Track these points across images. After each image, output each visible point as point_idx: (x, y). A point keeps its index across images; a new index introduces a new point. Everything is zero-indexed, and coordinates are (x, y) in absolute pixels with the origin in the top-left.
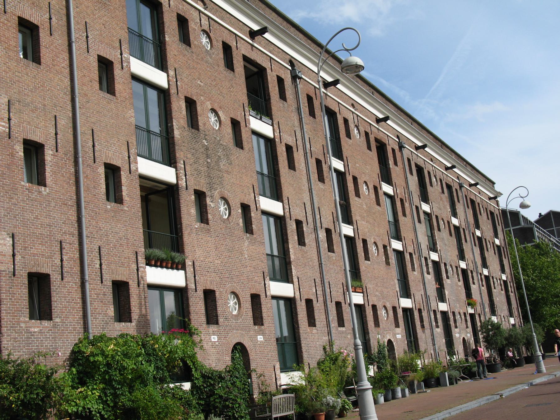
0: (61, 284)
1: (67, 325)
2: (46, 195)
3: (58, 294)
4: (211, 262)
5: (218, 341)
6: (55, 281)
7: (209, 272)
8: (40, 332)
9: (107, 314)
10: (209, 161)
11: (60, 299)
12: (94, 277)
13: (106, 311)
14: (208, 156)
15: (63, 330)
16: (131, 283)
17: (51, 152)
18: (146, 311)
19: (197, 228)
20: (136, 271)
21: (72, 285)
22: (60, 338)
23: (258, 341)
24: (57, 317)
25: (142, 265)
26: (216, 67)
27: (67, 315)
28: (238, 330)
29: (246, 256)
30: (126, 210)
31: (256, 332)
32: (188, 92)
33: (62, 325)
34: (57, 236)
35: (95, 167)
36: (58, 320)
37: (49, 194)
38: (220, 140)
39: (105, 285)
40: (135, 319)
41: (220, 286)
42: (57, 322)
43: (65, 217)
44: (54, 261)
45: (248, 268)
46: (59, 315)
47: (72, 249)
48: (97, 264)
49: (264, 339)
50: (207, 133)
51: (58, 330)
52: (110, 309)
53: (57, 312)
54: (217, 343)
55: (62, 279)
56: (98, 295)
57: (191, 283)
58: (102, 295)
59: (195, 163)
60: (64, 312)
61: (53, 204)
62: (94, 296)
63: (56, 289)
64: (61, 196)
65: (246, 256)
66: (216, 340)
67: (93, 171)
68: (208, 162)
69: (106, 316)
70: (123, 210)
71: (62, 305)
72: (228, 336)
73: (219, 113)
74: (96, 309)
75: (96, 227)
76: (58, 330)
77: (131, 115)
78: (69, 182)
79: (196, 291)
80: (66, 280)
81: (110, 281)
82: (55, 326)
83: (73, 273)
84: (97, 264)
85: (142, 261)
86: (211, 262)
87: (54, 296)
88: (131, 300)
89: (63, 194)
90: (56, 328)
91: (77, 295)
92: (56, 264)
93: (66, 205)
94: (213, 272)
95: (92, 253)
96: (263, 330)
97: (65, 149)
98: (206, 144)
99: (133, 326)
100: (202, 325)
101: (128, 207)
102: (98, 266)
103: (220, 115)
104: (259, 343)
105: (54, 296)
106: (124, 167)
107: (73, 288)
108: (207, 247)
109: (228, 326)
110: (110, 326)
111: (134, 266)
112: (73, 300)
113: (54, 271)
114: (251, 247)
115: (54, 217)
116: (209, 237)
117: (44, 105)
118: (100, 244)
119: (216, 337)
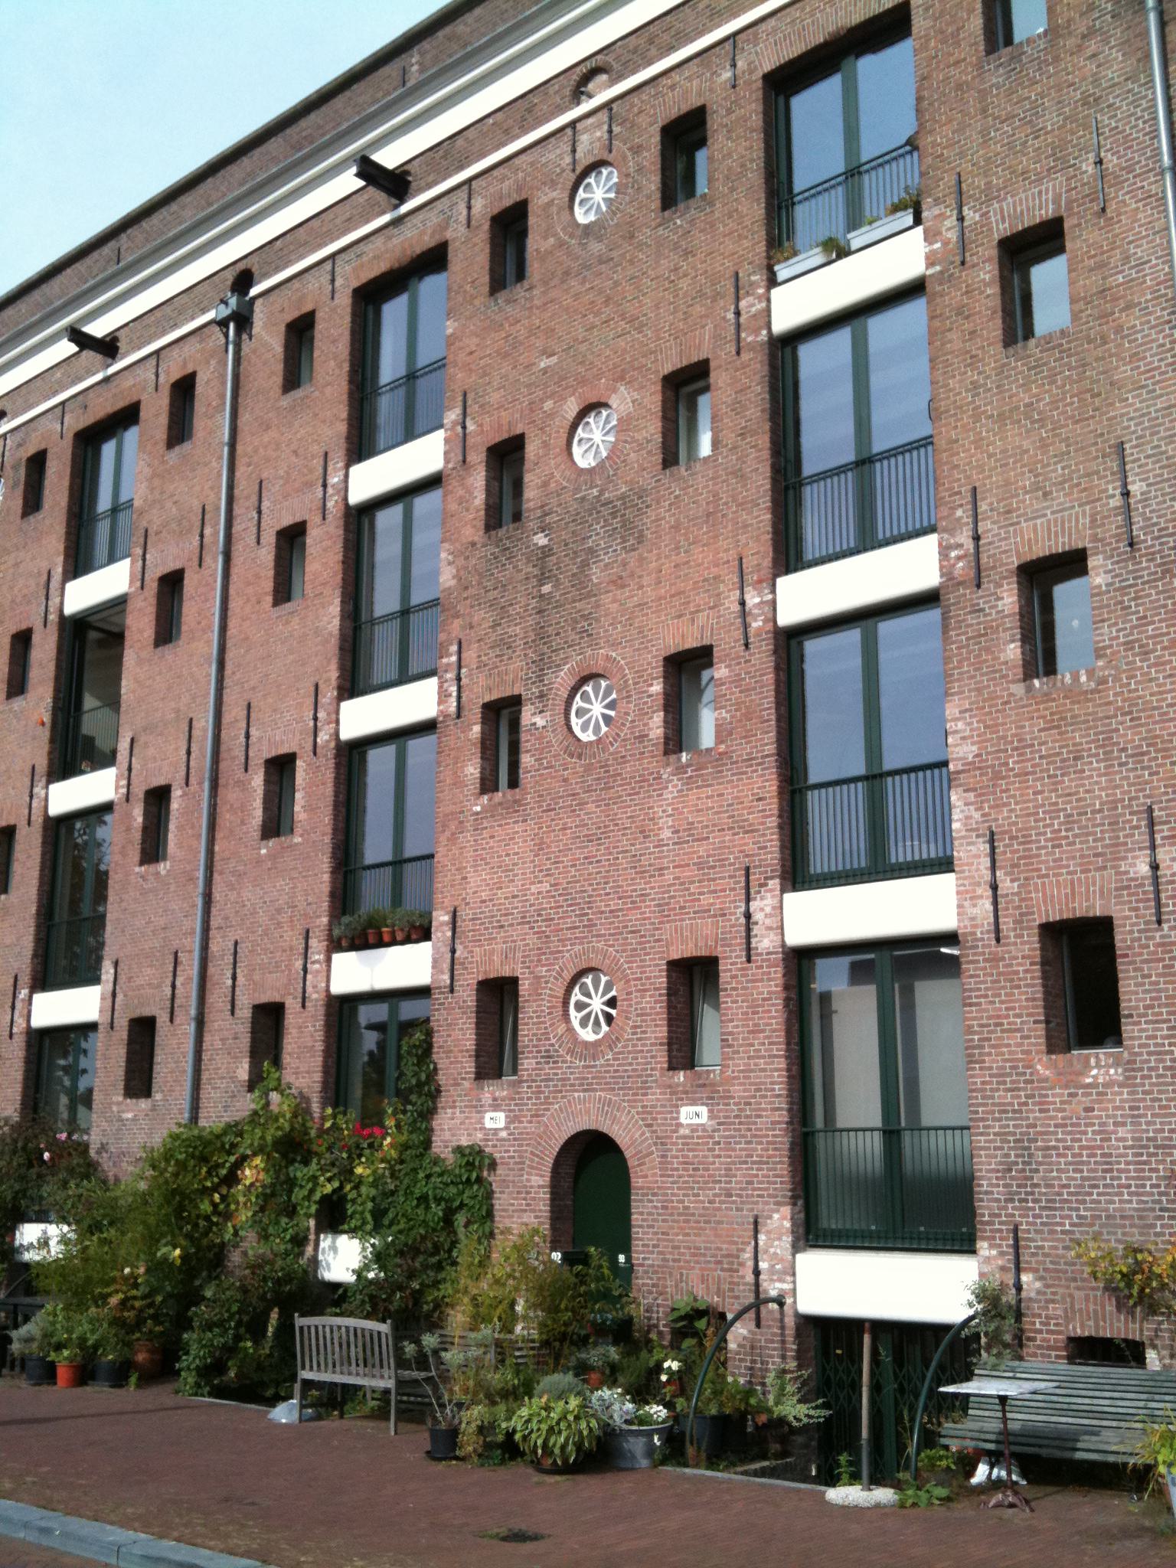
4: (514, 897)
5: (506, 1128)
7: (502, 927)
8: (135, 1119)
19: (477, 813)
23: (679, 1125)
28: (595, 1090)
31: (671, 1094)
45: (669, 877)
49: (710, 1118)
54: (504, 1134)
65: (666, 834)
68: (541, 596)
72: (548, 1110)
79: (452, 991)
80: (177, 1021)
82: (154, 1108)
86: (514, 897)
94: (519, 924)
96: (713, 1085)
104: (682, 1131)
108: (508, 855)
109: (552, 1080)
114: (693, 795)
116: (516, 822)
118: (239, 934)
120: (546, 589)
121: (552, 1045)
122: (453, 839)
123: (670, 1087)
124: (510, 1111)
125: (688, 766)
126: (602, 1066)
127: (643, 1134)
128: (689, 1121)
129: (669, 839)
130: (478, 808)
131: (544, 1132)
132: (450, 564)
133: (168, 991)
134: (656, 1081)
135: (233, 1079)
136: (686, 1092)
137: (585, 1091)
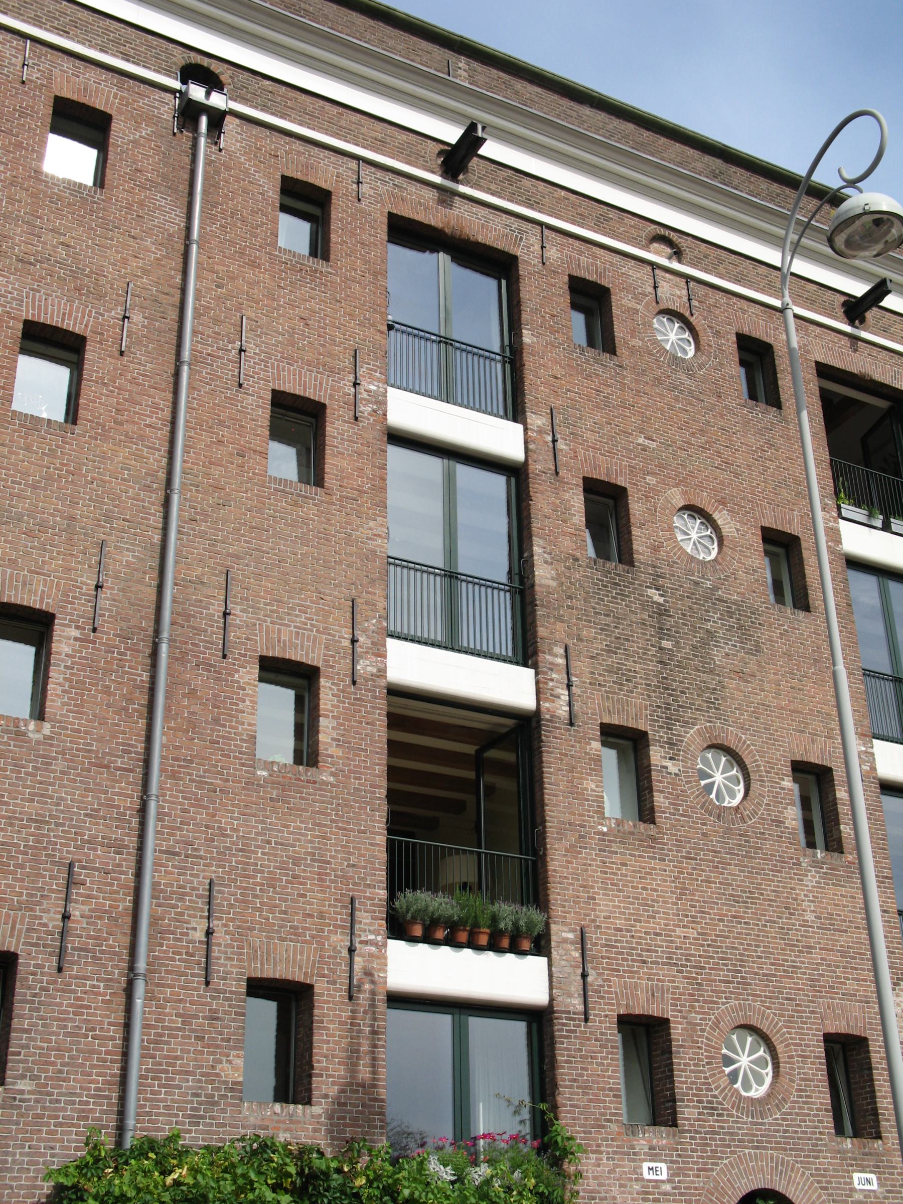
0: (55, 982)
1: (58, 1101)
2: (38, 742)
3: (38, 1010)
4: (657, 934)
5: (669, 1181)
6: (34, 974)
7: (644, 962)
9: (218, 1075)
10: (667, 644)
11: (44, 1025)
12: (179, 967)
13: (213, 1067)
14: (662, 633)
15: (38, 1116)
16: (320, 987)
17: (75, 633)
18: (374, 1073)
19: (604, 834)
20: (345, 953)
21: (94, 986)
22: (24, 1140)
23: (853, 1190)
24: (23, 1077)
25: (371, 937)
26: (713, 400)
27: (60, 1071)
28: (765, 1148)
29: (810, 917)
30: (327, 783)
31: (842, 1159)
32: (596, 467)
33: (37, 1101)
34: (61, 851)
35: (225, 668)
36: (24, 1085)
37: (51, 738)
38: (715, 588)
39: (217, 991)
40: (326, 1096)
41: (693, 1007)
42: (22, 1092)
43: (99, 798)
44: (41, 918)
45: (817, 955)
46: (30, 1070)
47: (112, 885)
48: (195, 929)
49: (880, 1185)
50: (665, 570)
51: (21, 1115)
52: (229, 1062)
53: (26, 1062)
54: (667, 1187)
55: (60, 970)
56: (187, 1018)
57: (570, 995)
58: (204, 1018)
59: (609, 651)
60: (53, 1064)
61: (59, 765)
62: (171, 1021)
63: (35, 995)
64: (91, 745)
66: (664, 1177)
67: (217, 679)
68: (661, 649)
69: (212, 1082)
70: (315, 782)
71: (50, 1041)
72: (717, 1164)
73: (716, 516)
74: (176, 1058)
75: (207, 827)
76: (21, 1115)
77: (375, 532)
78: (126, 709)
79: (586, 1020)
81: (239, 980)
83: (102, 952)
84: (195, 929)
85: (371, 924)
86: (657, 934)
87: (22, 1016)
88: (315, 1038)
89: (100, 740)
90: (12, 1107)
91: (108, 1017)
92: (45, 925)
93: (107, 767)
94: (664, 964)
95: (180, 900)
96: (877, 1155)
97: (124, 624)
98: (661, 600)
99: (313, 1116)
100: (603, 1127)
101: (333, 774)
102: (199, 935)
103: (719, 522)
104: (858, 1197)
105: (22, 1016)
106: (332, 667)
107: (98, 994)
108: (644, 889)
109: (718, 1133)
110: (224, 1111)
111: (340, 940)
112: (93, 1029)
113: (36, 945)
114: (830, 890)
115: (61, 799)
116: (654, 858)
117: (72, 518)
118: (214, 872)
119: (663, 1166)
120: (667, 644)
121: (715, 1096)
122: (572, 850)
123: (839, 1152)
124: (672, 1162)
125: (823, 863)
126: (770, 1124)
127: (820, 1196)
128: (861, 1187)
129: (813, 921)
130: (605, 829)
131: (715, 1188)
132: (546, 562)
133: (53, 921)
134: (825, 1145)
135: (211, 1077)
136: (855, 1159)
137: (757, 1148)
